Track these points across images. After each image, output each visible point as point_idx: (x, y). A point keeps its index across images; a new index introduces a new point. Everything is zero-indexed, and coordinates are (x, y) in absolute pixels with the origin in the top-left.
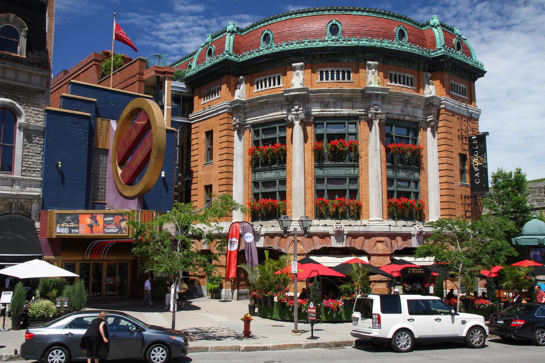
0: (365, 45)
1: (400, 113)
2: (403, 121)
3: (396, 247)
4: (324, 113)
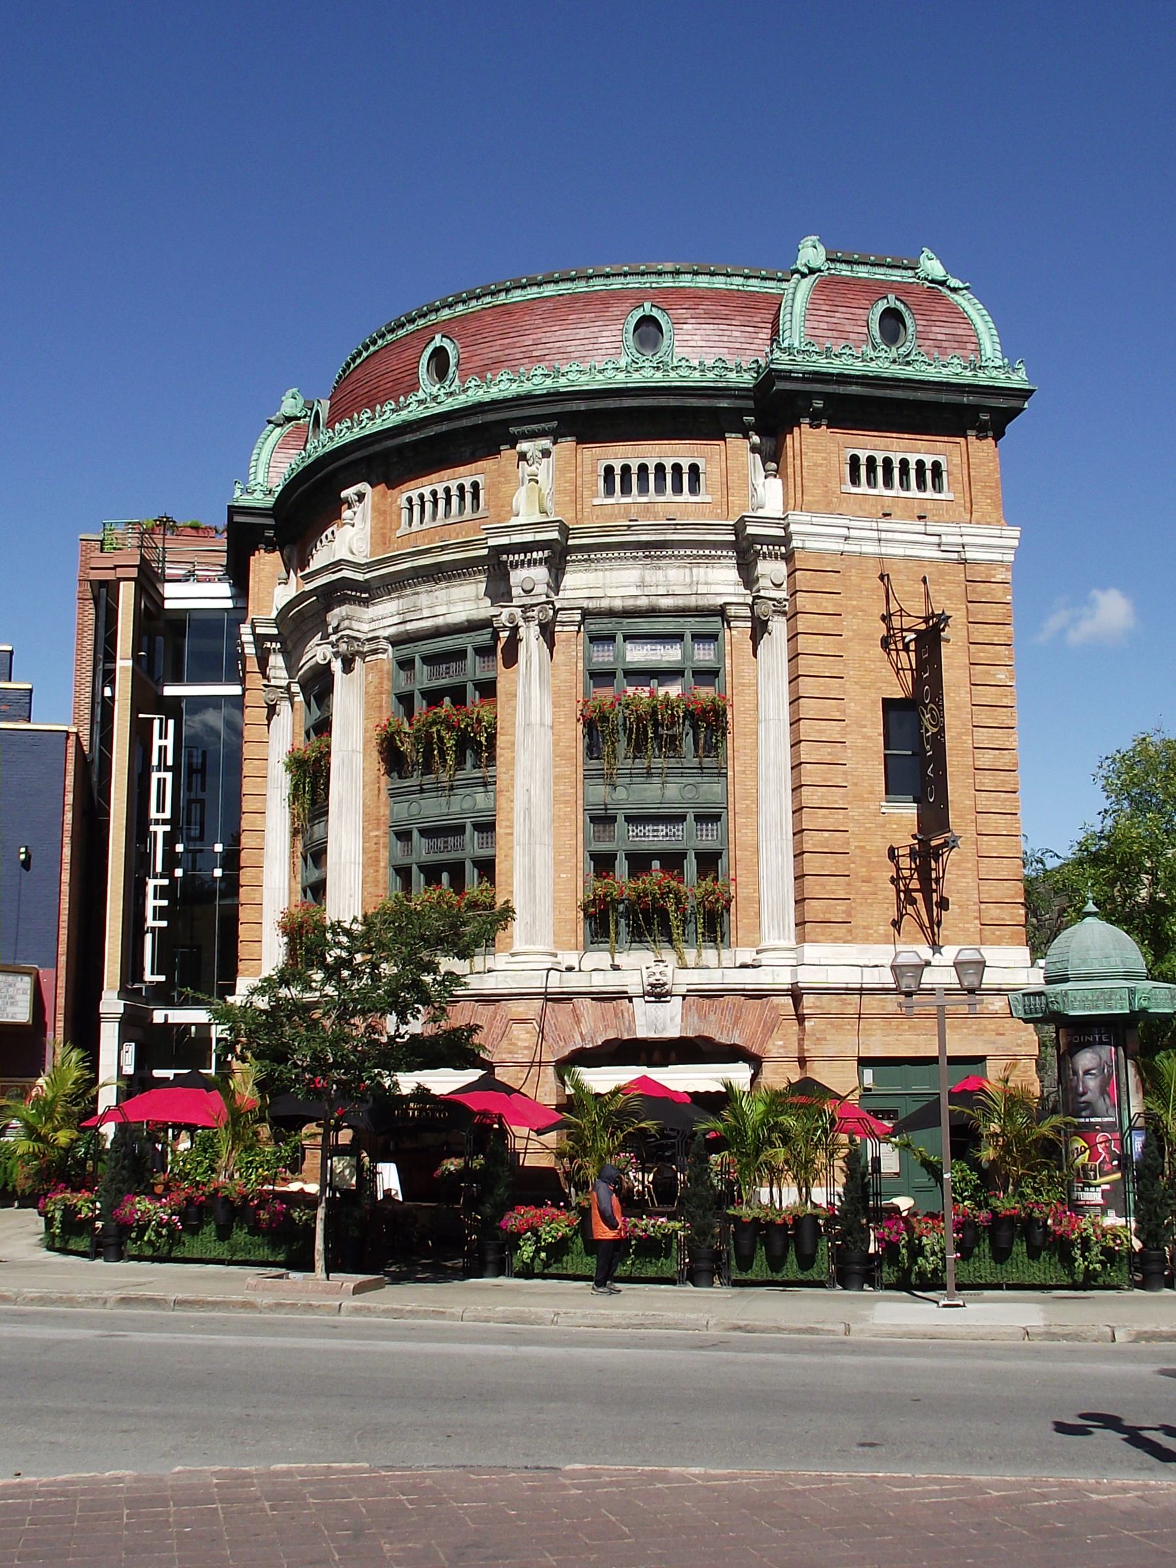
0: (501, 396)
1: (634, 591)
2: (652, 612)
3: (578, 1038)
4: (409, 626)
